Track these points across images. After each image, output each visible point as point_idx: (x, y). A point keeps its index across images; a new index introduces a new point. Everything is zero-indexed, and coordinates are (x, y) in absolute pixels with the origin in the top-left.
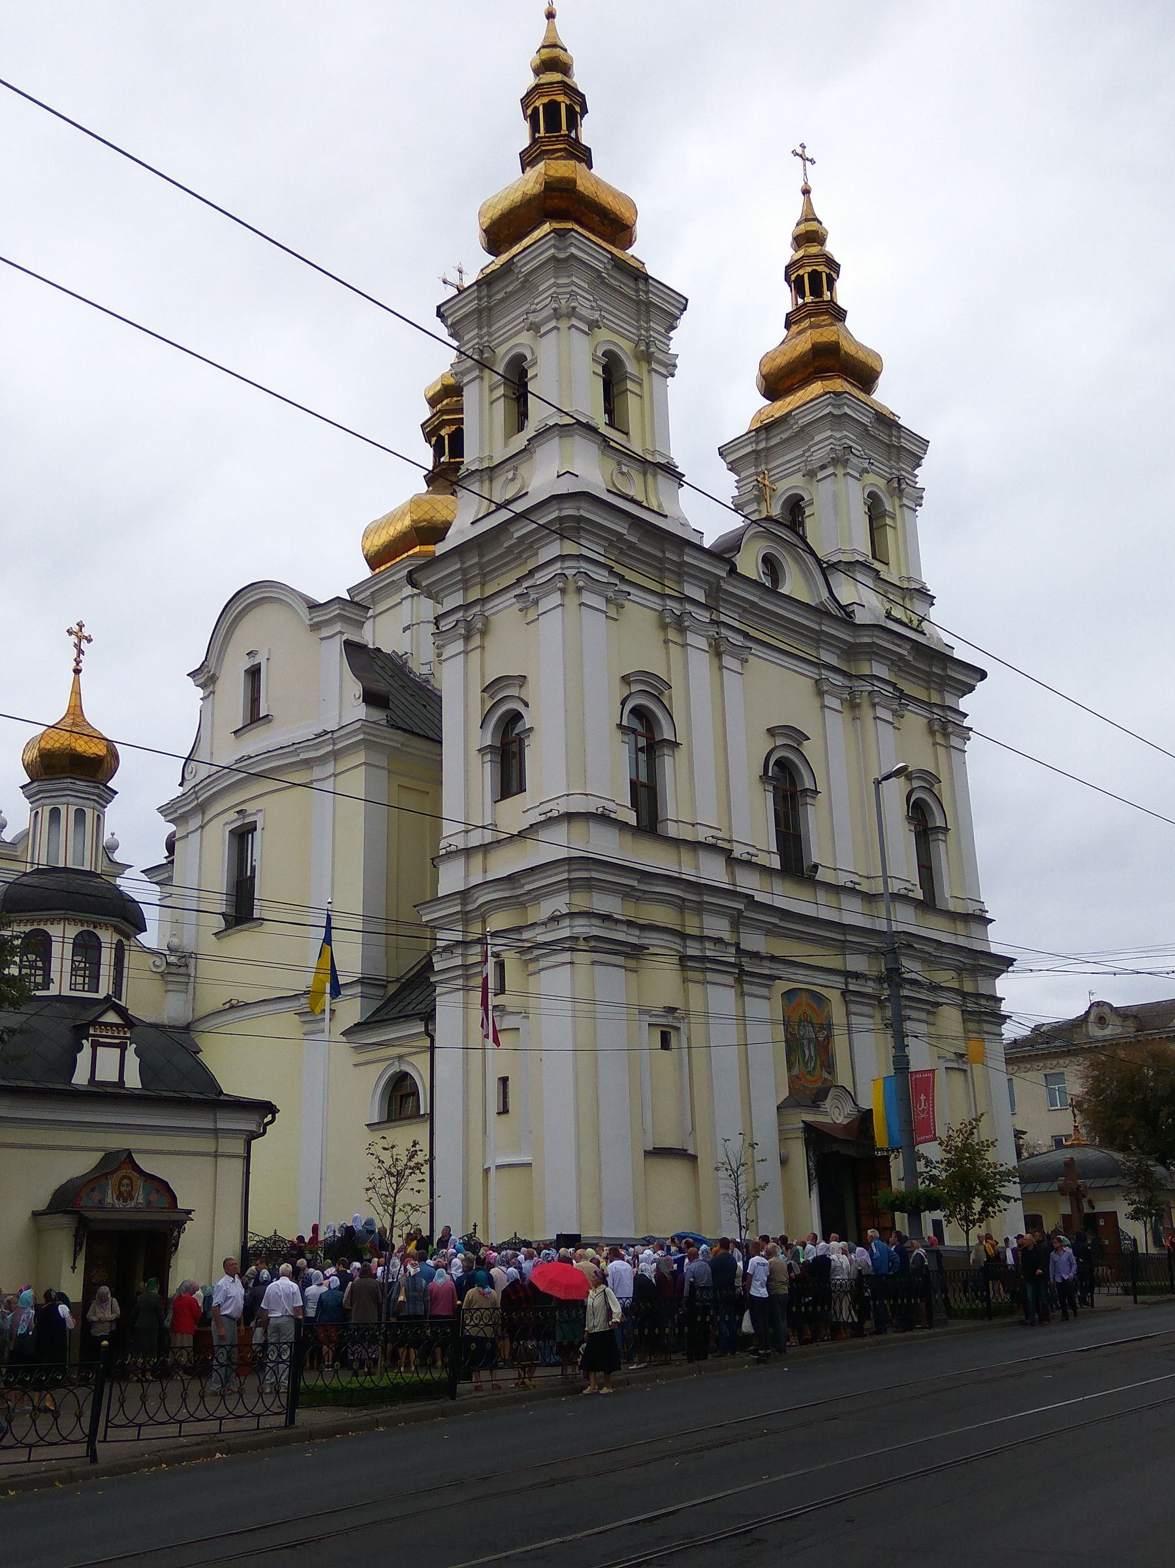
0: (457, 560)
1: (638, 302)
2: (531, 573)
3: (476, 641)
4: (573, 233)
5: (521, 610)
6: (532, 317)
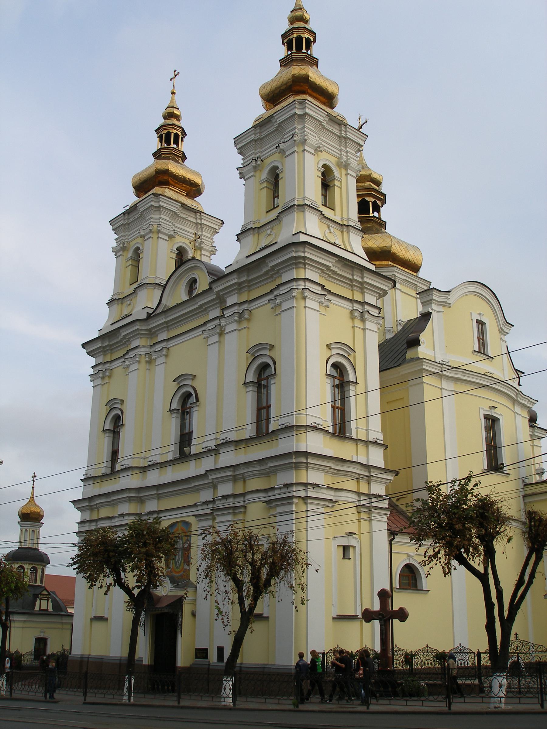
0: (100, 342)
1: (197, 224)
2: (128, 351)
3: (106, 380)
4: (161, 196)
5: (124, 368)
6: (142, 233)
